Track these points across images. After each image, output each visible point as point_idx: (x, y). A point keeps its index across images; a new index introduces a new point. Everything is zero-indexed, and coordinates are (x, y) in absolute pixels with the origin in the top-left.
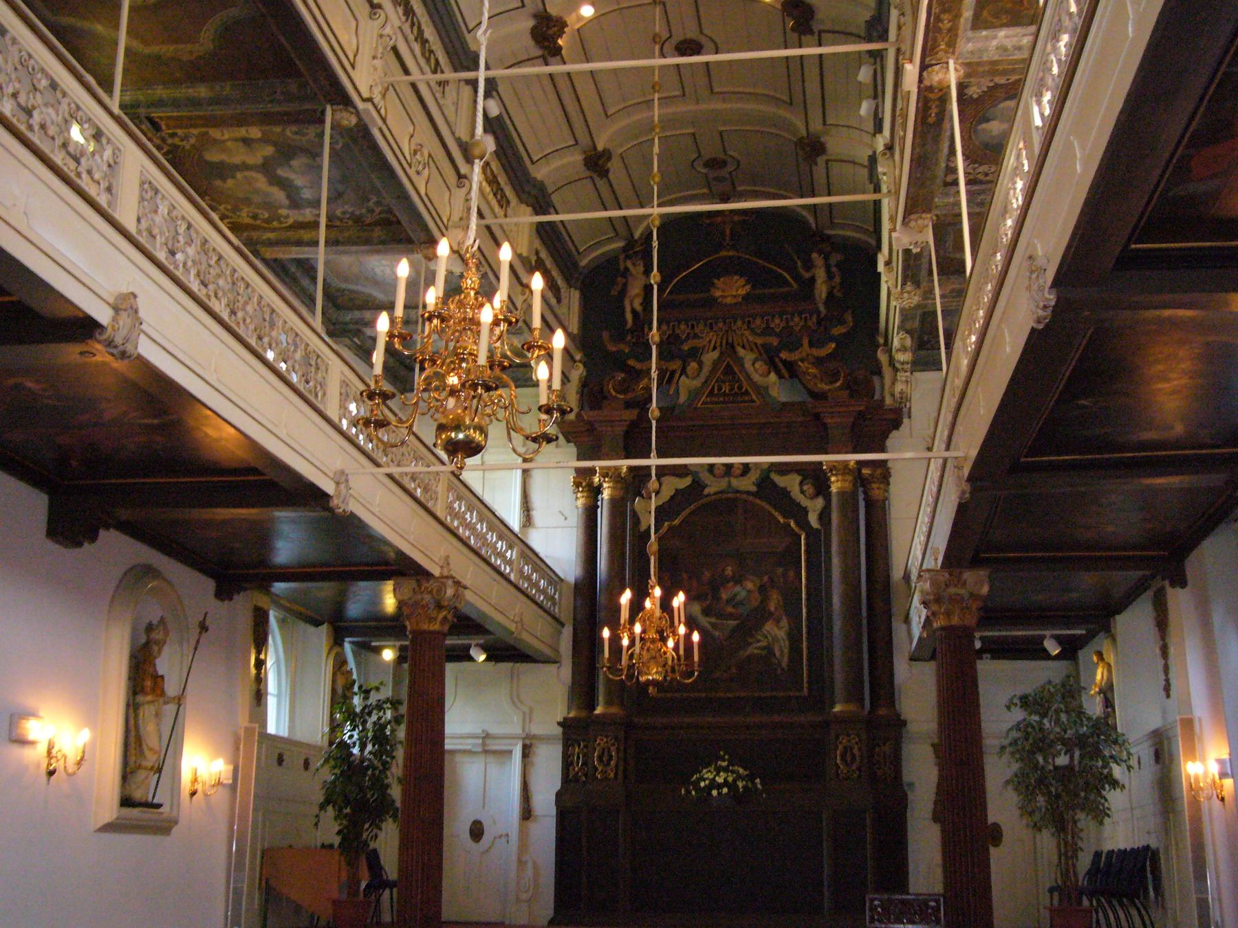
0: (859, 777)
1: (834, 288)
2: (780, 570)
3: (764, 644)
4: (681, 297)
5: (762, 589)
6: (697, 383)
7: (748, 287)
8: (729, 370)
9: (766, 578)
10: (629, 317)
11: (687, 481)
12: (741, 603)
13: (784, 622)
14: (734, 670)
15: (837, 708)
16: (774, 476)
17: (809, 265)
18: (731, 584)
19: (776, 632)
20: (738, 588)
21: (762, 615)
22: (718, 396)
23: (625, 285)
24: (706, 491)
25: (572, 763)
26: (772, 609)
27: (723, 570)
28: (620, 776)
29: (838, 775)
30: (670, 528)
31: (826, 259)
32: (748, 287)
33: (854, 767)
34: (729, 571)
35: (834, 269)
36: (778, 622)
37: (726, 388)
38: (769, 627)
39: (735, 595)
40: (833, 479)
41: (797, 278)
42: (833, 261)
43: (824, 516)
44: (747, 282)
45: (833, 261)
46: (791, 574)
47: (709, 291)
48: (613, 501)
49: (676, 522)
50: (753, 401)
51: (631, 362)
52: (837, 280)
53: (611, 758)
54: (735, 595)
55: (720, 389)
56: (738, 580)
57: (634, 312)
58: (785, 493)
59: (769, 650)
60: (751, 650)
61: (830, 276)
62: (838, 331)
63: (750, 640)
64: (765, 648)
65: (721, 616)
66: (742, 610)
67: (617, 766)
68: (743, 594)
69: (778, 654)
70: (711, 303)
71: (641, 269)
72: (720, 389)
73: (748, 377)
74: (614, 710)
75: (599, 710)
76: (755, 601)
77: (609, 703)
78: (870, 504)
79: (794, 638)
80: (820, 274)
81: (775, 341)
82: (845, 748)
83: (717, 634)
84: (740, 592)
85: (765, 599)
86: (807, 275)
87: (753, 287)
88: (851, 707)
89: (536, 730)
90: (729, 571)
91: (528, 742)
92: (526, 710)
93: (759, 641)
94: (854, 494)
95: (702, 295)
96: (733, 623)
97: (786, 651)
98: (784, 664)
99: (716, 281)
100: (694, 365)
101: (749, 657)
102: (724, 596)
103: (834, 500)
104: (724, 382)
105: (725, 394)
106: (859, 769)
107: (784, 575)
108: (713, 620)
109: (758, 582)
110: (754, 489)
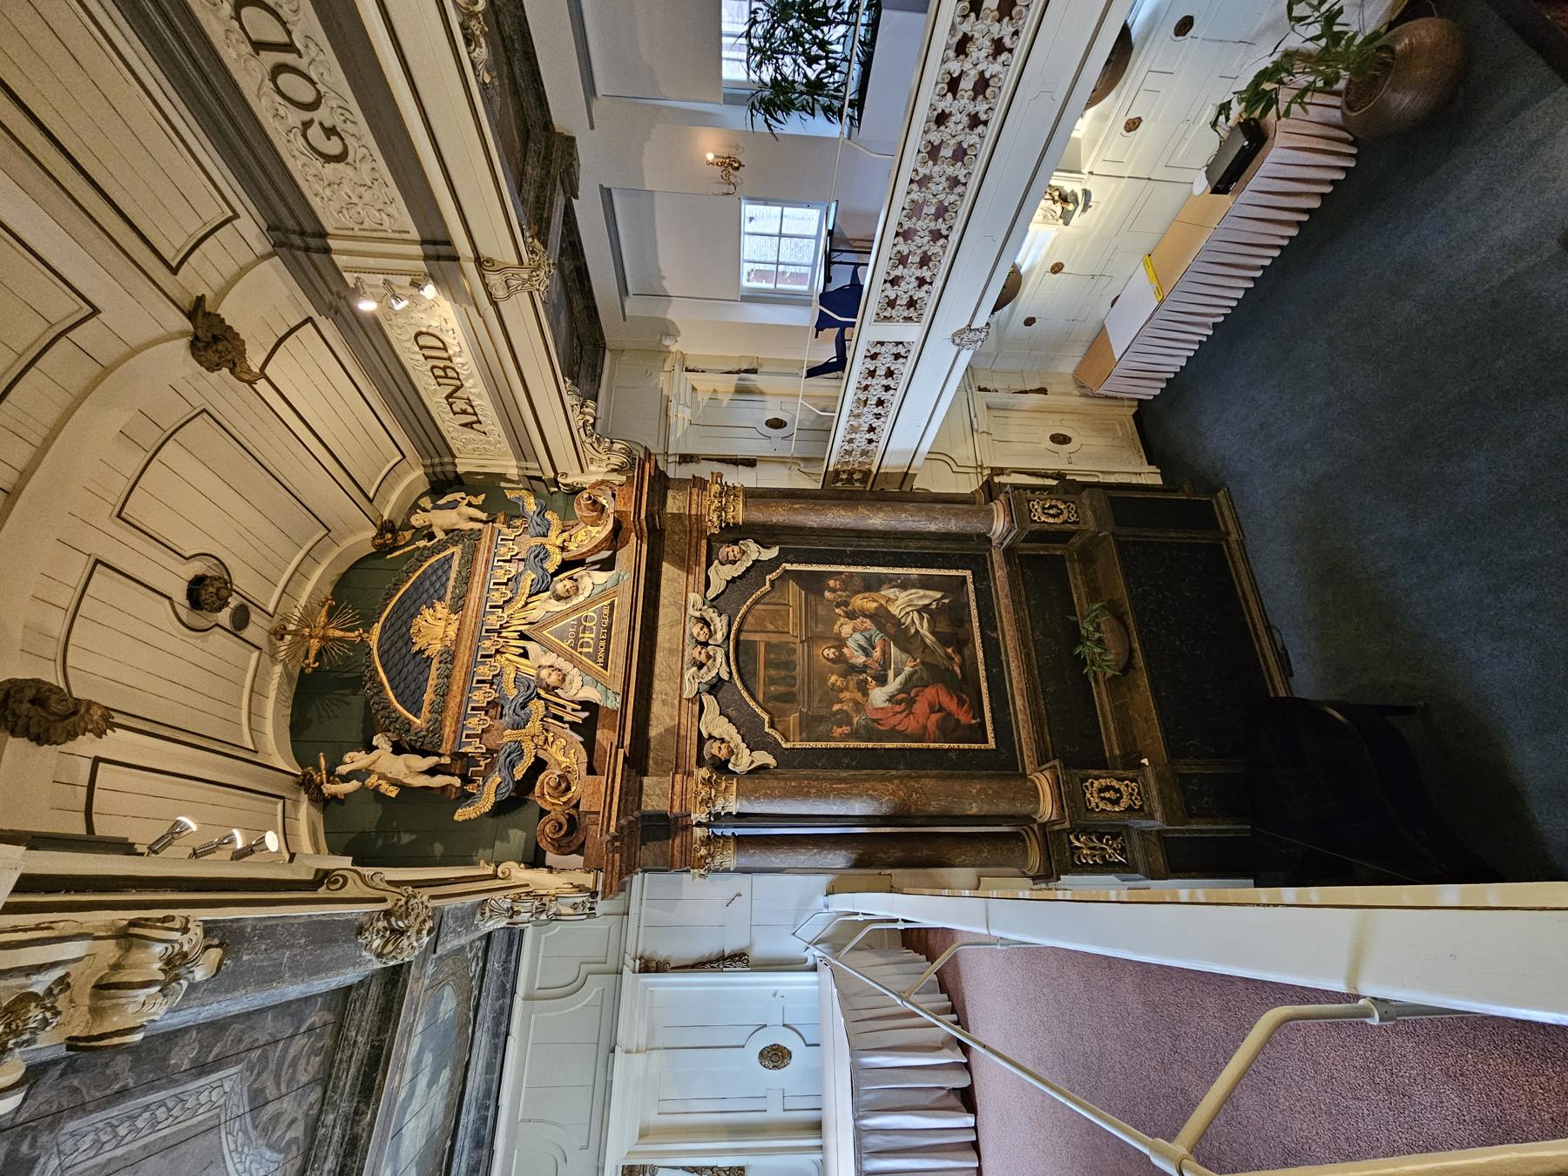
2: (827, 594)
4: (428, 697)
5: (851, 616)
6: (574, 674)
7: (438, 606)
10: (439, 781)
11: (708, 699)
12: (869, 640)
13: (890, 592)
15: (999, 525)
16: (711, 594)
18: (845, 650)
19: (903, 603)
20: (850, 643)
21: (881, 618)
24: (725, 677)
28: (1131, 774)
30: (772, 726)
32: (438, 606)
34: (831, 653)
36: (889, 600)
38: (894, 610)
39: (860, 646)
41: (443, 546)
44: (432, 606)
46: (832, 583)
50: (612, 604)
51: (519, 772)
53: (1108, 788)
54: (860, 646)
56: (840, 643)
57: (432, 772)
59: (922, 610)
61: (453, 505)
64: (922, 618)
65: (885, 665)
67: (1121, 780)
69: (927, 602)
70: (449, 656)
73: (575, 610)
79: (905, 584)
80: (442, 520)
81: (530, 576)
83: (908, 669)
84: (854, 643)
86: (440, 535)
87: (440, 599)
88: (998, 508)
90: (831, 653)
97: (921, 592)
98: (938, 595)
99: (416, 648)
101: (933, 633)
102: (860, 659)
107: (833, 590)
108: (891, 673)
110: (725, 618)
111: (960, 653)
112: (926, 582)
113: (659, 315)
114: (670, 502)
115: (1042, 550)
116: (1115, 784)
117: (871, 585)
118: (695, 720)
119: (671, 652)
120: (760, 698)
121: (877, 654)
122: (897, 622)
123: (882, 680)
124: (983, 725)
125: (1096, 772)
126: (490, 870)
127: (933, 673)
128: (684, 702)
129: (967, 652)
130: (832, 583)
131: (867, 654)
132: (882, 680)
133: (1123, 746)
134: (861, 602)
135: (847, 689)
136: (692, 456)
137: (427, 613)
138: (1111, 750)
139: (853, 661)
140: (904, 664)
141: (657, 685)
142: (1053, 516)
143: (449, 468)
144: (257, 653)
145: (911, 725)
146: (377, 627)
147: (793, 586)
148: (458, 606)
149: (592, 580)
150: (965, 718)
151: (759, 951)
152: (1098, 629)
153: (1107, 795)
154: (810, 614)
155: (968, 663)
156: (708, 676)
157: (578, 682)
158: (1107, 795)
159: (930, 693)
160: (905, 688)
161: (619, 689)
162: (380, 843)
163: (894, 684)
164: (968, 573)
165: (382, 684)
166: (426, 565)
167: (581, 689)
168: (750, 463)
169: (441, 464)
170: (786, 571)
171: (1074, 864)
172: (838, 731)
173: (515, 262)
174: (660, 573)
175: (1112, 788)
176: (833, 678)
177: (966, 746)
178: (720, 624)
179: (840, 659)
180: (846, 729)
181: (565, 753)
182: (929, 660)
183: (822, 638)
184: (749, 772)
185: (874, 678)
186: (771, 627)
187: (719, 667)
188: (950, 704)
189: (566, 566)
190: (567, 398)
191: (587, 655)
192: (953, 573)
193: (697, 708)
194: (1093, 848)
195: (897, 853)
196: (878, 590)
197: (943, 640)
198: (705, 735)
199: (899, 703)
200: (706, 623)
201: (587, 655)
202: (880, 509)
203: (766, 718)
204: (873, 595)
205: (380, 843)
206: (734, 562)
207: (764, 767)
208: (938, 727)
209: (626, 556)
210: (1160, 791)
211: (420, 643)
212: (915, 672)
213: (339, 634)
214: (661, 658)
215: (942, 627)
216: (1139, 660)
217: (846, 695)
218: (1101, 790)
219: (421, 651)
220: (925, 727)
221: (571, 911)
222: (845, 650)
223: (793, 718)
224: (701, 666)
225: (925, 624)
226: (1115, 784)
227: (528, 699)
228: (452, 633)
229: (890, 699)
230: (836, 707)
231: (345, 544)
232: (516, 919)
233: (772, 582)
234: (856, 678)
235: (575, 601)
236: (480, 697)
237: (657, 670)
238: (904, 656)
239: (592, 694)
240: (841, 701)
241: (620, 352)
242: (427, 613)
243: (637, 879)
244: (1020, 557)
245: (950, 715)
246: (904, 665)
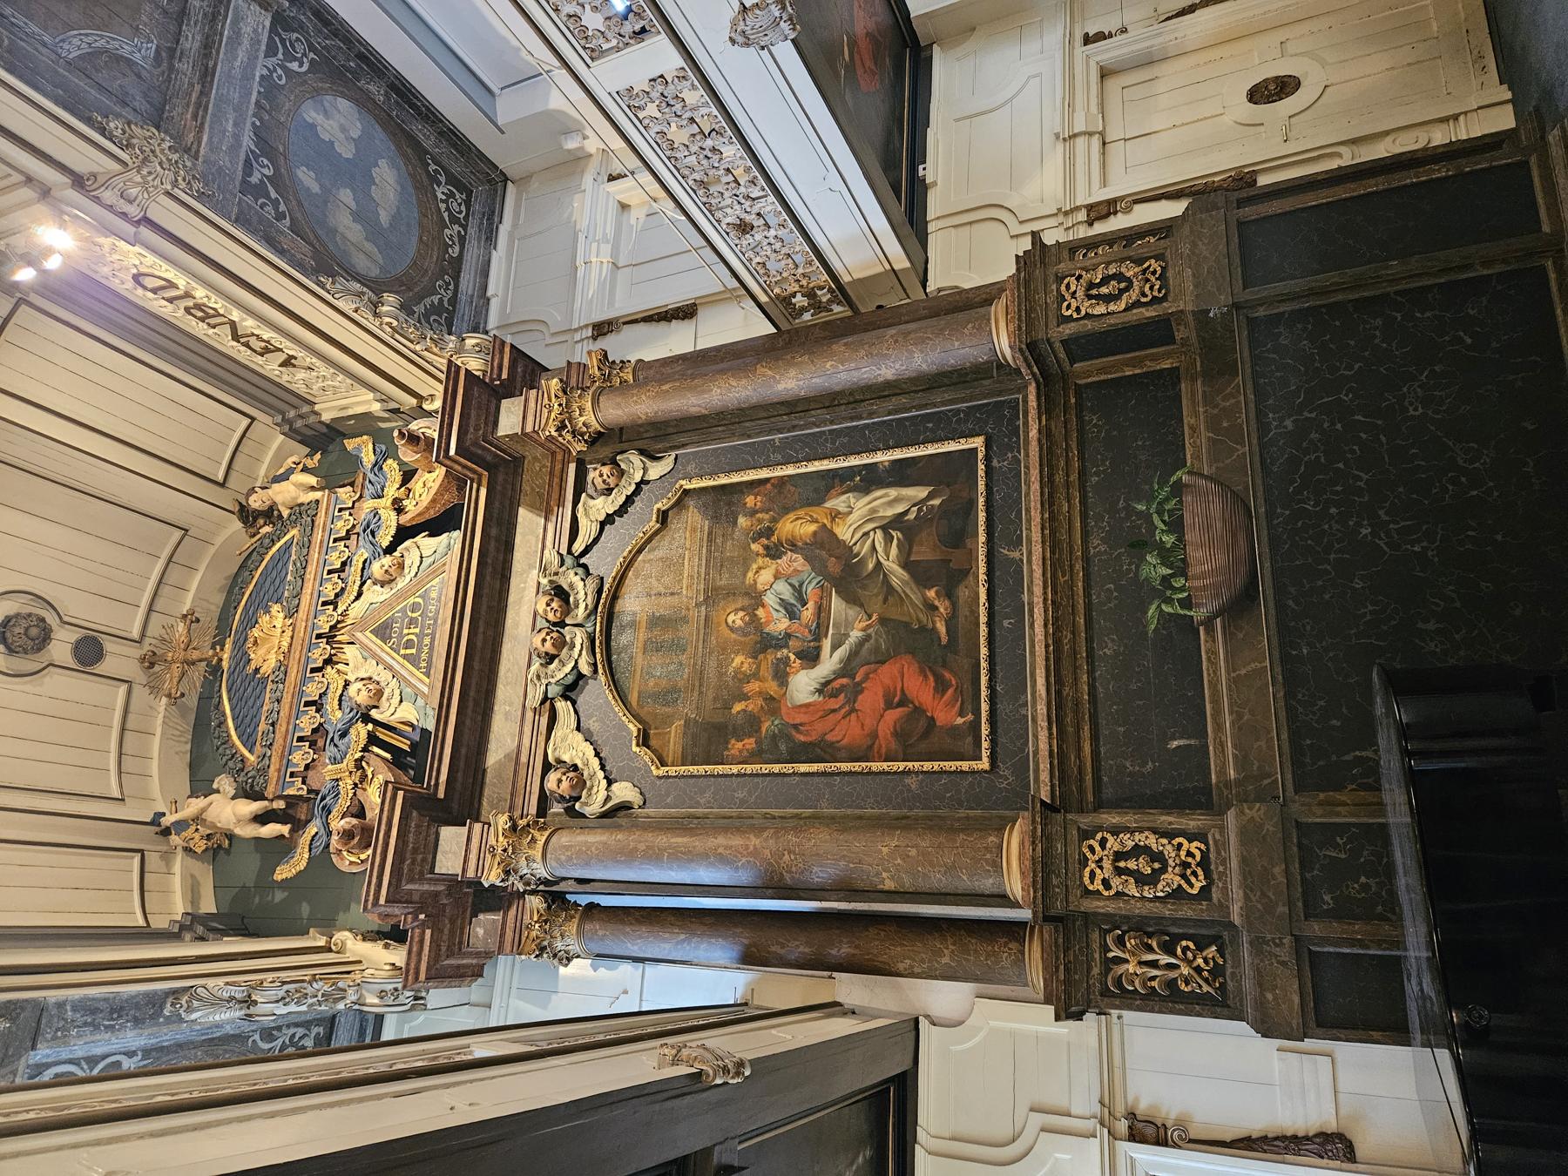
0: (1157, 258)
2: (742, 521)
3: (879, 534)
4: (262, 727)
5: (774, 552)
7: (276, 608)
9: (755, 547)
11: (562, 706)
12: (798, 591)
13: (838, 502)
14: (931, 594)
16: (578, 547)
18: (760, 612)
20: (770, 599)
21: (824, 547)
22: (419, 650)
24: (585, 669)
25: (1171, 984)
26: (813, 528)
27: (731, 629)
28: (1193, 823)
29: (1155, 300)
32: (276, 608)
33: (1130, 271)
34: (737, 619)
36: (835, 515)
38: (844, 532)
46: (750, 500)
53: (1137, 851)
57: (262, 819)
60: (892, 565)
62: (368, 458)
63: (871, 566)
64: (888, 539)
65: (819, 633)
66: (810, 590)
67: (1170, 835)
68: (783, 588)
69: (900, 509)
74: (1015, 841)
76: (794, 562)
79: (870, 479)
82: (1090, 297)
83: (855, 635)
89: (1084, 1101)
91: (1122, 1126)
92: (1037, 1119)
93: (873, 548)
96: (836, 603)
97: (893, 492)
98: (921, 492)
101: (906, 565)
102: (780, 624)
105: (420, 636)
106: (1138, 261)
107: (753, 513)
108: (827, 644)
109: (760, 561)
110: (592, 585)
111: (949, 594)
112: (901, 474)
113: (539, 108)
115: (1125, 366)
118: (542, 739)
120: (633, 698)
122: (844, 552)
123: (810, 657)
124: (975, 726)
125: (1114, 819)
126: (322, 942)
127: (902, 638)
128: (530, 715)
129: (963, 593)
131: (792, 615)
132: (810, 657)
133: (1242, 761)
134: (798, 526)
135: (756, 676)
136: (609, 323)
138: (1222, 771)
139: (770, 629)
140: (849, 625)
142: (1108, 299)
143: (312, 419)
144: (123, 688)
145: (847, 732)
147: (693, 518)
150: (947, 715)
152: (1176, 526)
153: (1132, 865)
154: (714, 560)
155: (964, 611)
156: (561, 672)
158: (1132, 865)
159: (888, 673)
160: (846, 669)
162: (257, 900)
163: (830, 662)
164: (978, 442)
165: (224, 714)
166: (268, 558)
168: (686, 312)
169: (301, 416)
170: (686, 492)
171: (1105, 993)
172: (736, 746)
173: (117, 167)
175: (1147, 850)
176: (738, 660)
177: (936, 766)
178: (582, 593)
180: (750, 743)
182: (894, 614)
183: (731, 593)
184: (604, 815)
185: (799, 655)
188: (921, 690)
189: (404, 533)
190: (340, 304)
192: (951, 446)
193: (544, 721)
194: (1153, 964)
195: (799, 947)
196: (819, 502)
197: (919, 573)
198: (550, 759)
199: (834, 695)
202: (791, 364)
204: (816, 512)
205: (257, 900)
206: (609, 491)
207: (625, 807)
208: (895, 734)
210: (1244, 861)
212: (867, 638)
215: (925, 552)
216: (1265, 587)
217: (753, 687)
218: (1119, 856)
220: (874, 735)
221: (376, 1001)
222: (760, 612)
224: (550, 658)
225: (894, 551)
226: (1151, 841)
227: (351, 723)
228: (285, 644)
230: (738, 707)
231: (219, 541)
232: (252, 1010)
234: (771, 657)
235: (401, 583)
236: (307, 723)
238: (852, 612)
240: (745, 697)
241: (527, 179)
244: (1079, 390)
245: (918, 710)
246: (852, 624)
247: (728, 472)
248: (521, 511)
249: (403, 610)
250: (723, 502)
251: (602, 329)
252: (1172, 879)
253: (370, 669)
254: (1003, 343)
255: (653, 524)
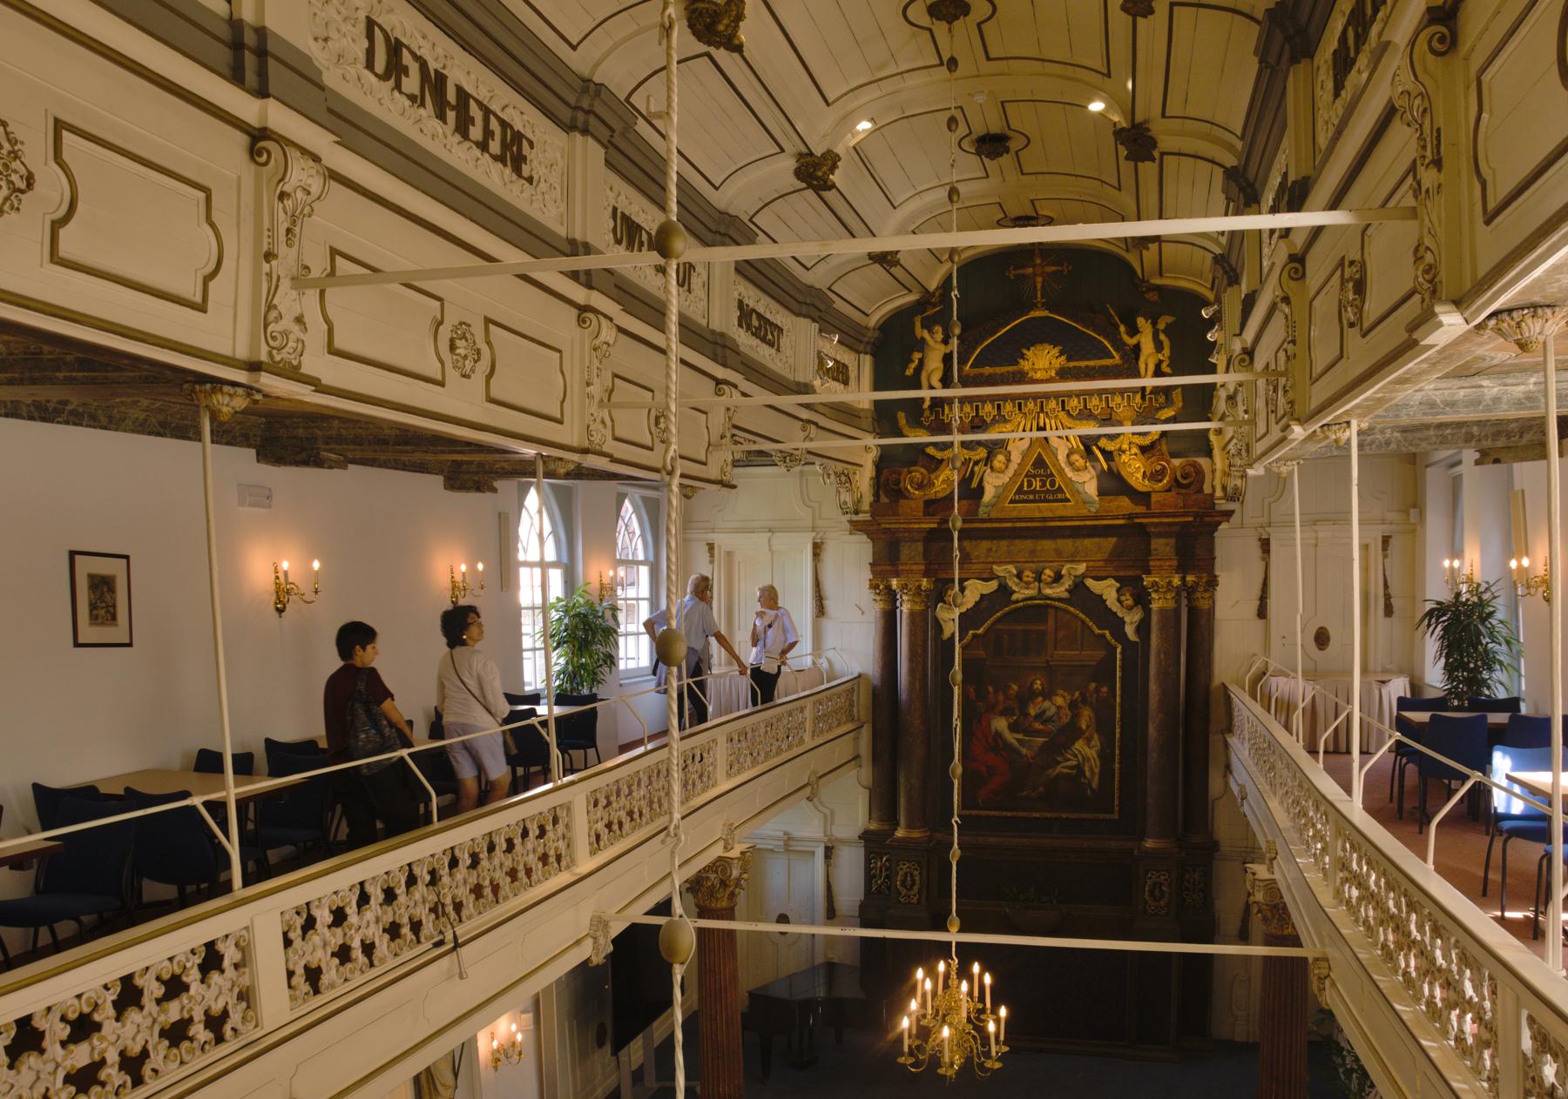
1: (1161, 362)
2: (1093, 685)
4: (987, 370)
5: (1073, 705)
6: (1006, 478)
8: (1040, 463)
11: (994, 585)
12: (1050, 720)
13: (1096, 741)
16: (1090, 582)
17: (1133, 331)
19: (1086, 751)
20: (1047, 704)
21: (1071, 733)
23: (921, 361)
24: (1014, 597)
30: (974, 636)
31: (1154, 324)
34: (1038, 685)
35: (1162, 337)
37: (1037, 484)
38: (1079, 745)
39: (1044, 712)
40: (1154, 595)
41: (1119, 345)
42: (1161, 326)
43: (1143, 628)
44: (1061, 353)
45: (1161, 326)
46: (1105, 689)
47: (1017, 363)
48: (912, 614)
49: (980, 631)
52: (1167, 351)
53: (913, 881)
54: (1044, 712)
55: (1030, 484)
56: (1048, 694)
58: (1100, 599)
59: (1079, 768)
61: (1159, 347)
64: (1072, 768)
67: (919, 892)
71: (939, 337)
72: (1030, 484)
73: (1061, 472)
74: (916, 834)
75: (900, 833)
77: (910, 826)
78: (1193, 611)
79: (1105, 757)
80: (1146, 341)
83: (1024, 751)
85: (1076, 717)
86: (1131, 341)
87: (1069, 359)
90: (1038, 685)
94: (1177, 612)
95: (1010, 369)
97: (1097, 770)
100: (1001, 458)
102: (1032, 712)
103: (1154, 619)
104: (1034, 476)
105: (1034, 492)
107: (1097, 690)
108: (1020, 736)
110: (1066, 595)
114: (1162, 541)
116: (916, 888)
117: (1103, 725)
119: (1033, 552)
121: (1037, 726)
122: (1068, 745)
130: (1105, 689)
131: (1038, 717)
132: (1013, 728)
134: (1086, 718)
137: (1055, 351)
141: (1004, 544)
146: (1046, 313)
147: (1100, 654)
148: (1063, 375)
149: (1088, 482)
151: (829, 625)
156: (1012, 584)
157: (999, 482)
161: (994, 515)
163: (1010, 737)
167: (993, 484)
174: (1106, 536)
179: (1032, 695)
181: (947, 480)
186: (1061, 635)
187: (1021, 593)
191: (1022, 485)
200: (1058, 578)
201: (1022, 485)
203: (980, 631)
206: (1120, 601)
209: (1125, 504)
211: (1029, 354)
213: (1039, 286)
214: (1029, 544)
217: (1001, 698)
219: (1023, 356)
223: (981, 653)
228: (1039, 375)
229: (998, 734)
233: (1103, 636)
237: (1017, 542)
239: (988, 495)
240: (996, 692)
242: (1055, 351)
243: (864, 537)
247: (1122, 678)
248: (1114, 540)
249: (1052, 475)
250: (1103, 672)
251: (1265, 545)
252: (904, 892)
253: (1016, 458)
254: (1149, 844)
255: (1097, 631)
